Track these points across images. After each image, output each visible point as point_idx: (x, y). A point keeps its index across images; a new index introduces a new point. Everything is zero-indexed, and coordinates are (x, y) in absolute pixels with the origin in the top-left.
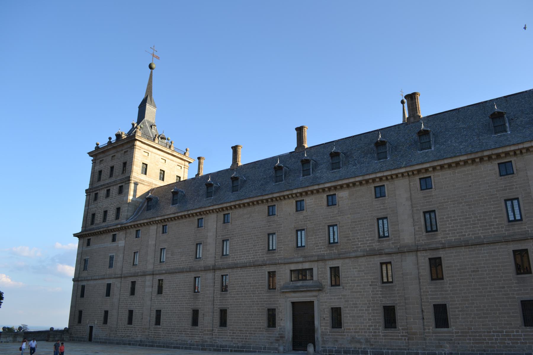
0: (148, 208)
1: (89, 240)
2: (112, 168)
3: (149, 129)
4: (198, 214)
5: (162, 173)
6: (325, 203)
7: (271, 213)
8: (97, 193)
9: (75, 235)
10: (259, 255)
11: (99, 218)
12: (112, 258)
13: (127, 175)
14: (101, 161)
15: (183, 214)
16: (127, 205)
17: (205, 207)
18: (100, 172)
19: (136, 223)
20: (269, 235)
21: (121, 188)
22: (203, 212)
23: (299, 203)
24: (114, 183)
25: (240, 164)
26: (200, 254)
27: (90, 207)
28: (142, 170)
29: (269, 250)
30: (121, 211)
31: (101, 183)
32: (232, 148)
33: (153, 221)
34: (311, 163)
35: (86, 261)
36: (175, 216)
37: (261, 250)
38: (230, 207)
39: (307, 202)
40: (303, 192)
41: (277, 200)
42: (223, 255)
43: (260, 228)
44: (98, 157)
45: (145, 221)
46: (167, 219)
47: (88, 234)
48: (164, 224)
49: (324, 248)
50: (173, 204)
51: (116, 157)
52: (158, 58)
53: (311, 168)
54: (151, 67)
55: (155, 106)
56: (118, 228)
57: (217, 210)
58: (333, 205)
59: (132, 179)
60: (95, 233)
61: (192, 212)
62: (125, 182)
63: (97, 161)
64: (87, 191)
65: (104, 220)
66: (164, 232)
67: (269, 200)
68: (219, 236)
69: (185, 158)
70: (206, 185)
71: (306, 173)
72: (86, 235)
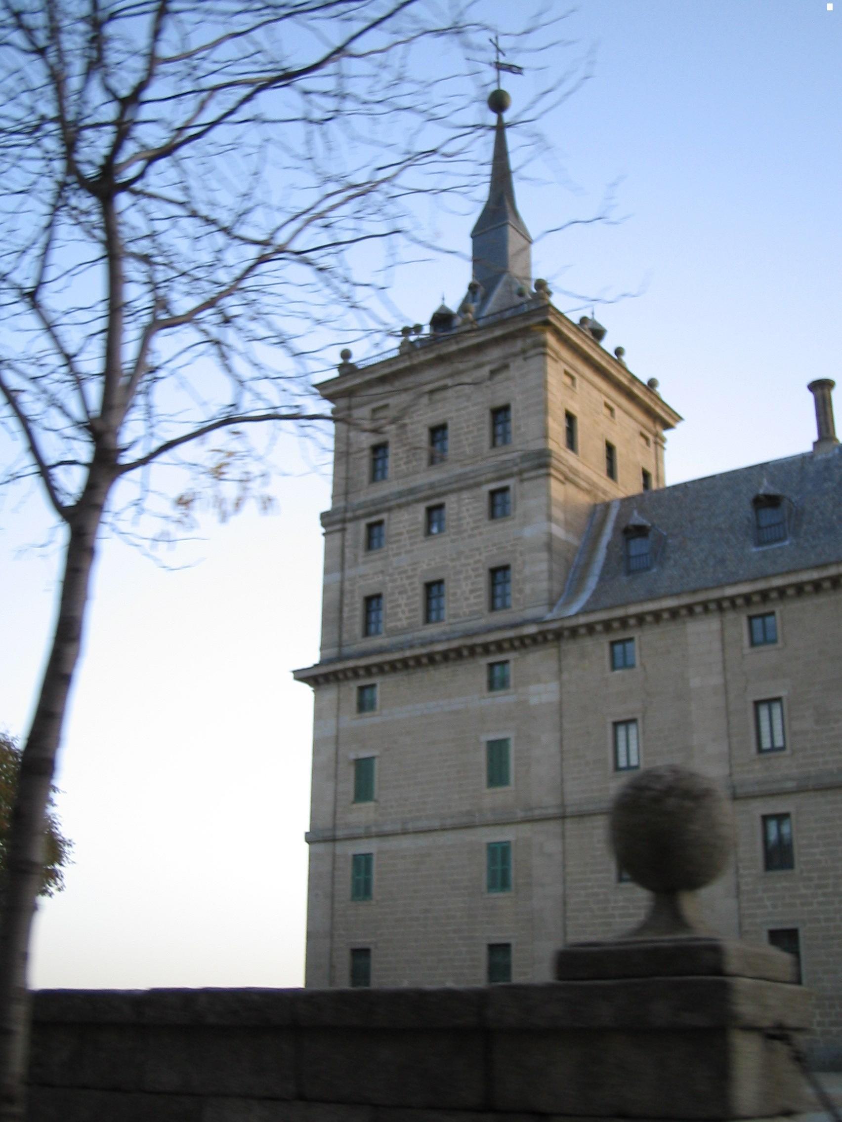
8: (380, 523)
9: (302, 676)
11: (403, 611)
12: (497, 751)
27: (349, 573)
30: (514, 575)
35: (363, 769)
46: (782, 591)
47: (368, 669)
56: (522, 639)
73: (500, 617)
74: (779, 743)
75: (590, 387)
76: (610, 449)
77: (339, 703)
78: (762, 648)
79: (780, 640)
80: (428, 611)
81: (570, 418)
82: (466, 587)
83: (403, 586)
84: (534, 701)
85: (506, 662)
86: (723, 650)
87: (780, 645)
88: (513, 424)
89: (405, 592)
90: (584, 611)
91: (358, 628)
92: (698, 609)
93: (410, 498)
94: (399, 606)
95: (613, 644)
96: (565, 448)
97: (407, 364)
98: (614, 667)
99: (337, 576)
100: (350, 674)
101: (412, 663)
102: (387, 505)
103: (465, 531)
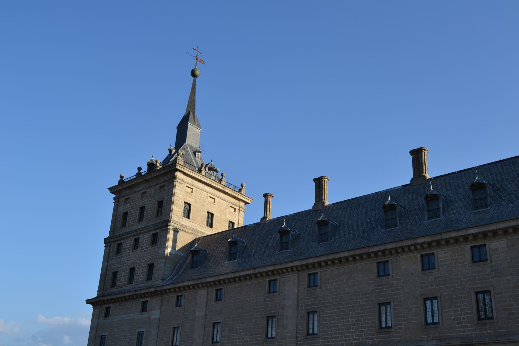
0: (194, 265)
1: (108, 309)
2: (142, 209)
3: (192, 156)
4: (270, 273)
5: (211, 216)
6: (469, 257)
7: (382, 271)
8: (121, 243)
9: (88, 302)
10: (366, 335)
11: (123, 278)
12: (140, 335)
13: (163, 219)
14: (126, 199)
15: (247, 273)
16: (163, 260)
17: (280, 264)
18: (125, 214)
19: (177, 285)
20: (380, 305)
21: (155, 236)
22: (277, 270)
23: (426, 259)
25: (327, 203)
26: (273, 331)
27: (110, 263)
28: (184, 213)
29: (381, 328)
30: (155, 268)
31: (127, 229)
32: (315, 180)
33: (202, 283)
34: (441, 200)
36: (235, 275)
37: (368, 327)
38: (319, 263)
39: (440, 256)
40: (434, 241)
41: (391, 253)
42: (308, 334)
43: (366, 294)
45: (191, 283)
47: (107, 300)
48: (218, 288)
49: (471, 326)
50: (230, 260)
52: (203, 62)
53: (441, 205)
54: (193, 74)
55: (199, 126)
56: (151, 293)
57: (299, 268)
58: (481, 261)
59: (171, 224)
60: (118, 298)
61: (261, 270)
62: (161, 228)
63: (120, 200)
65: (131, 280)
66: (218, 299)
67: (380, 254)
68: (302, 306)
69: (240, 197)
70: (280, 232)
71: (434, 214)
72: (104, 302)
73: (149, 283)
74: (218, 340)
82: (141, 271)
83: (124, 269)
84: (152, 317)
86: (207, 302)
87: (223, 301)
88: (163, 208)
90: (169, 284)
93: (130, 235)
94: (121, 277)
99: (106, 263)
101: (120, 300)
102: (123, 237)
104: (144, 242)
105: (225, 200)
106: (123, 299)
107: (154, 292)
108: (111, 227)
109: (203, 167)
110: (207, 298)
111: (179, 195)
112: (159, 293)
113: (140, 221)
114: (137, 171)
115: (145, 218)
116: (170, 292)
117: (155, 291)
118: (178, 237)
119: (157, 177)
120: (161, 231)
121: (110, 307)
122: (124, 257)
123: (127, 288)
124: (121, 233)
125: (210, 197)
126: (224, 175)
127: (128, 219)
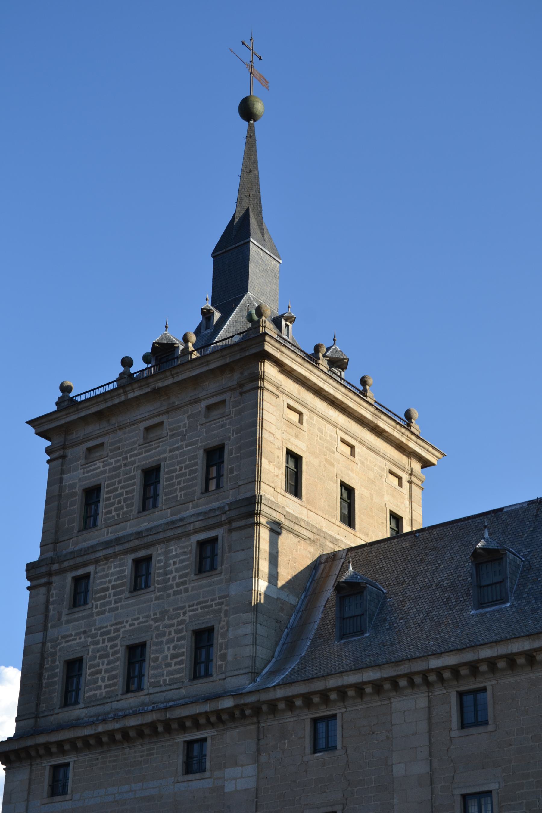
2: (151, 475)
8: (87, 576)
11: (103, 678)
13: (230, 495)
14: (90, 450)
16: (250, 616)
18: (92, 494)
19: (319, 686)
24: (175, 531)
27: (52, 633)
30: (218, 640)
31: (101, 534)
33: (409, 677)
44: (79, 433)
46: (492, 663)
47: (60, 744)
51: (165, 431)
52: (265, 83)
54: (247, 111)
56: (218, 713)
60: (98, 737)
62: (230, 521)
64: (32, 569)
65: (133, 678)
73: (202, 687)
75: (324, 422)
76: (348, 492)
77: (30, 784)
78: (472, 730)
79: (490, 722)
80: (129, 678)
81: (294, 458)
83: (104, 649)
84: (229, 787)
85: (204, 740)
86: (430, 731)
87: (490, 728)
88: (227, 466)
89: (107, 656)
91: (57, 698)
92: (403, 683)
93: (118, 548)
94: (99, 672)
95: (315, 721)
96: (283, 492)
97: (123, 398)
98: (315, 750)
99: (39, 637)
100: (42, 752)
101: (105, 739)
102: (92, 556)
103: (171, 587)
104: (172, 568)
105: (376, 452)
106: (118, 737)
107: (230, 712)
108: (45, 532)
109: (321, 355)
110: (429, 719)
111: (273, 429)
112: (250, 712)
113: (144, 508)
114: (121, 369)
115: (161, 499)
116: (412, 684)
117: (236, 706)
118: (280, 549)
119: (196, 380)
120: (230, 531)
121: (67, 765)
122: (99, 614)
123: (123, 704)
124: (85, 545)
125: (343, 441)
126: (370, 381)
127: (102, 505)
